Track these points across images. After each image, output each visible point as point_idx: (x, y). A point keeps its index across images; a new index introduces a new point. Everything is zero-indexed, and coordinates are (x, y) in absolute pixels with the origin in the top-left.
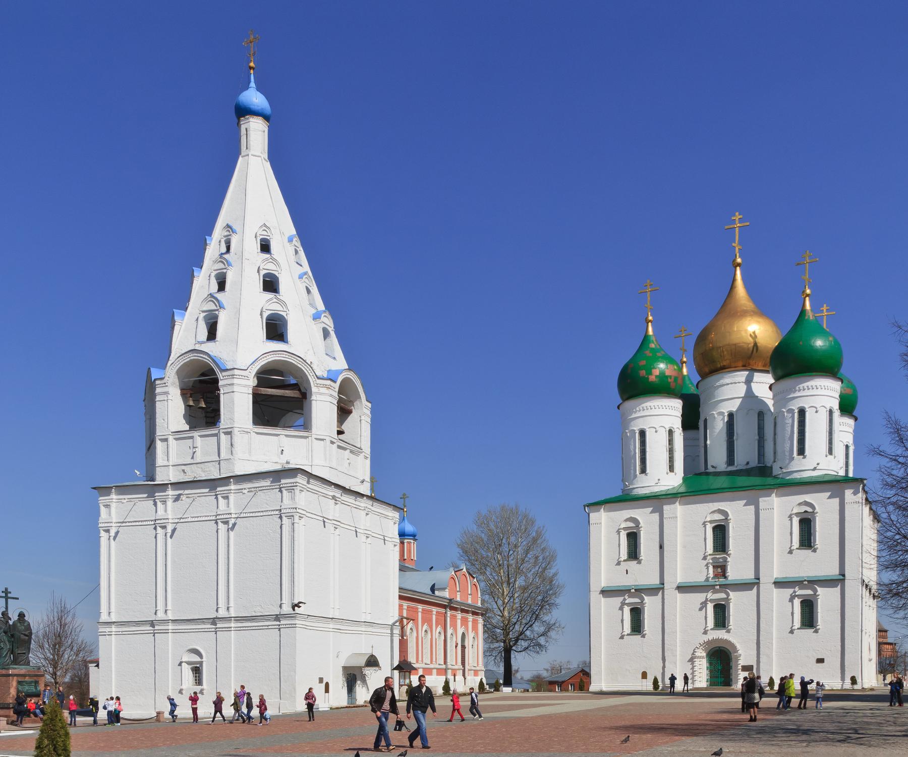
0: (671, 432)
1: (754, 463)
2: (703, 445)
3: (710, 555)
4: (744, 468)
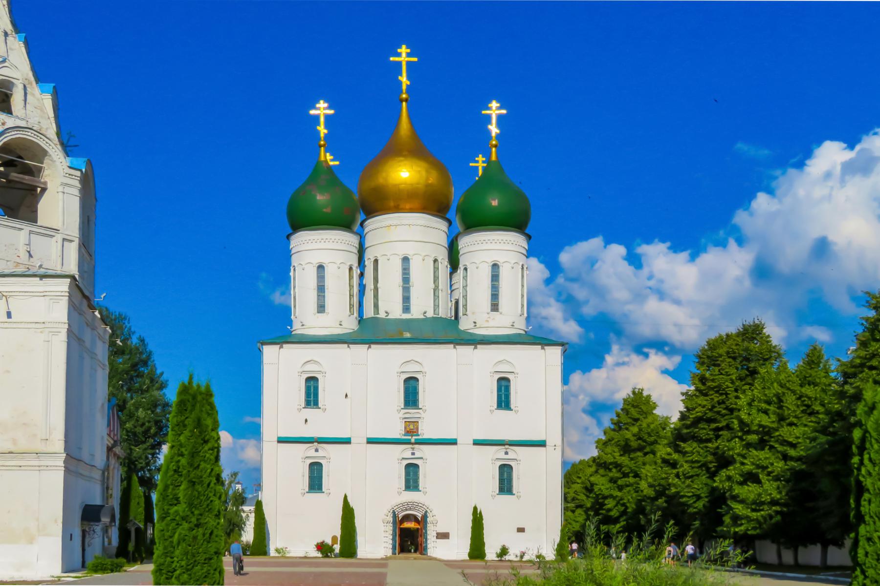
0: (351, 269)
1: (430, 314)
2: (372, 287)
3: (402, 409)
4: (422, 317)
